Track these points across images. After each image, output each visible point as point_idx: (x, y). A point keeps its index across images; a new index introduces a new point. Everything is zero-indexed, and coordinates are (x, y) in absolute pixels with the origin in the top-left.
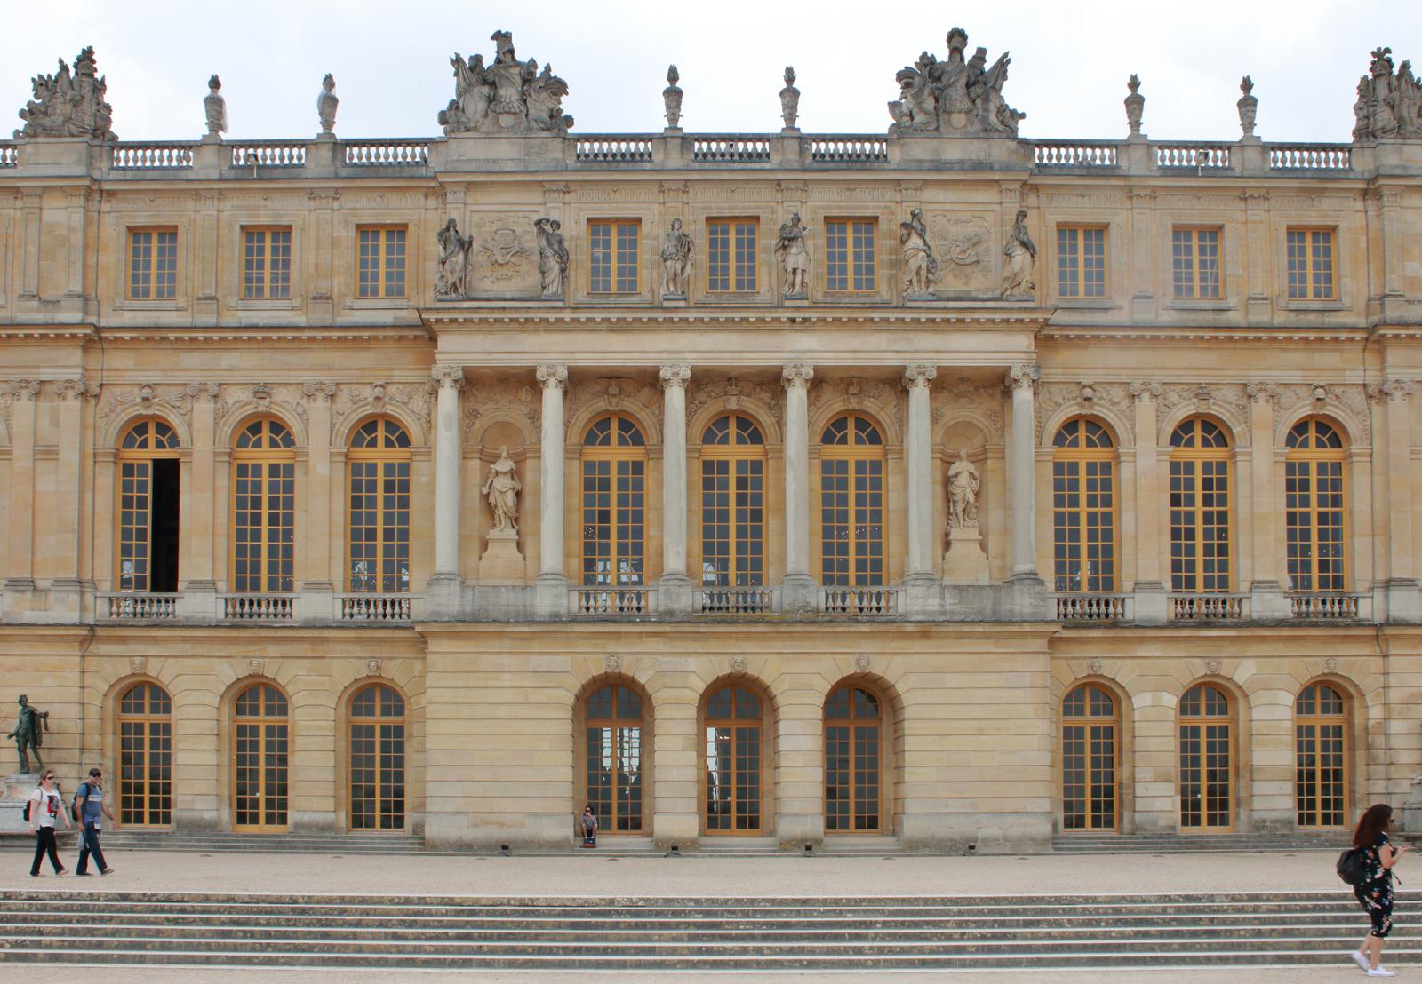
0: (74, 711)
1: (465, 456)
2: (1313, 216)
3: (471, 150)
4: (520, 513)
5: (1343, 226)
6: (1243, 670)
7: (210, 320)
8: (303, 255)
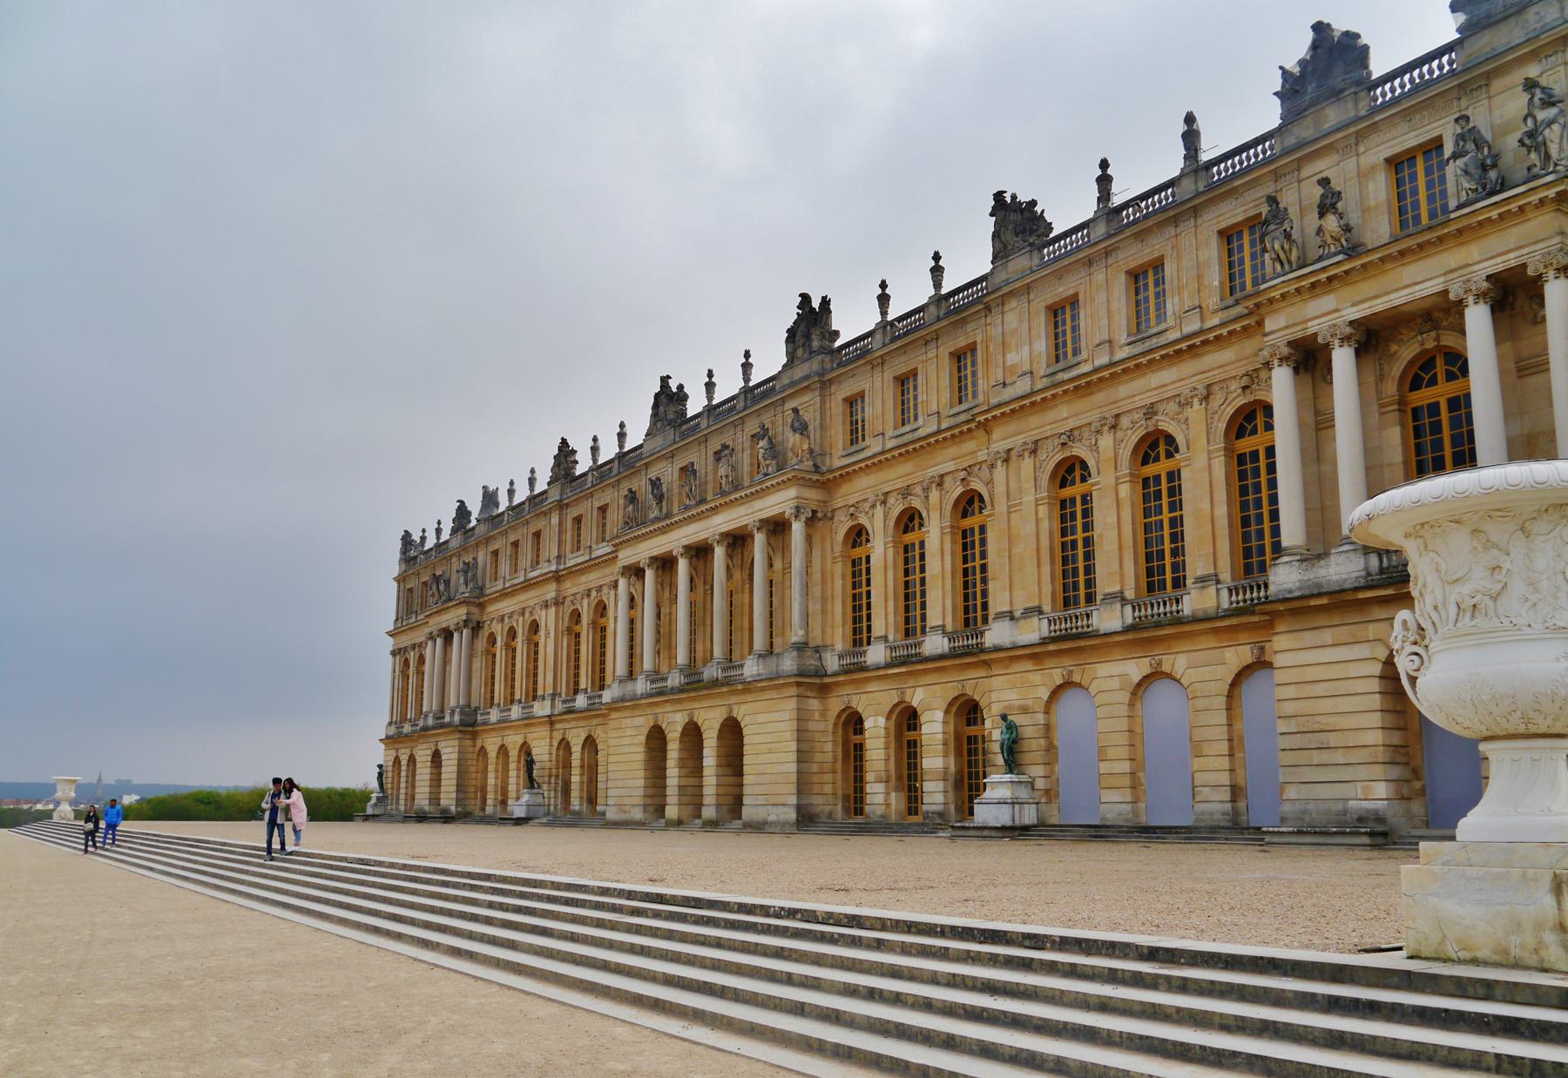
0: (546, 758)
2: (961, 342)
5: (979, 339)
6: (917, 698)
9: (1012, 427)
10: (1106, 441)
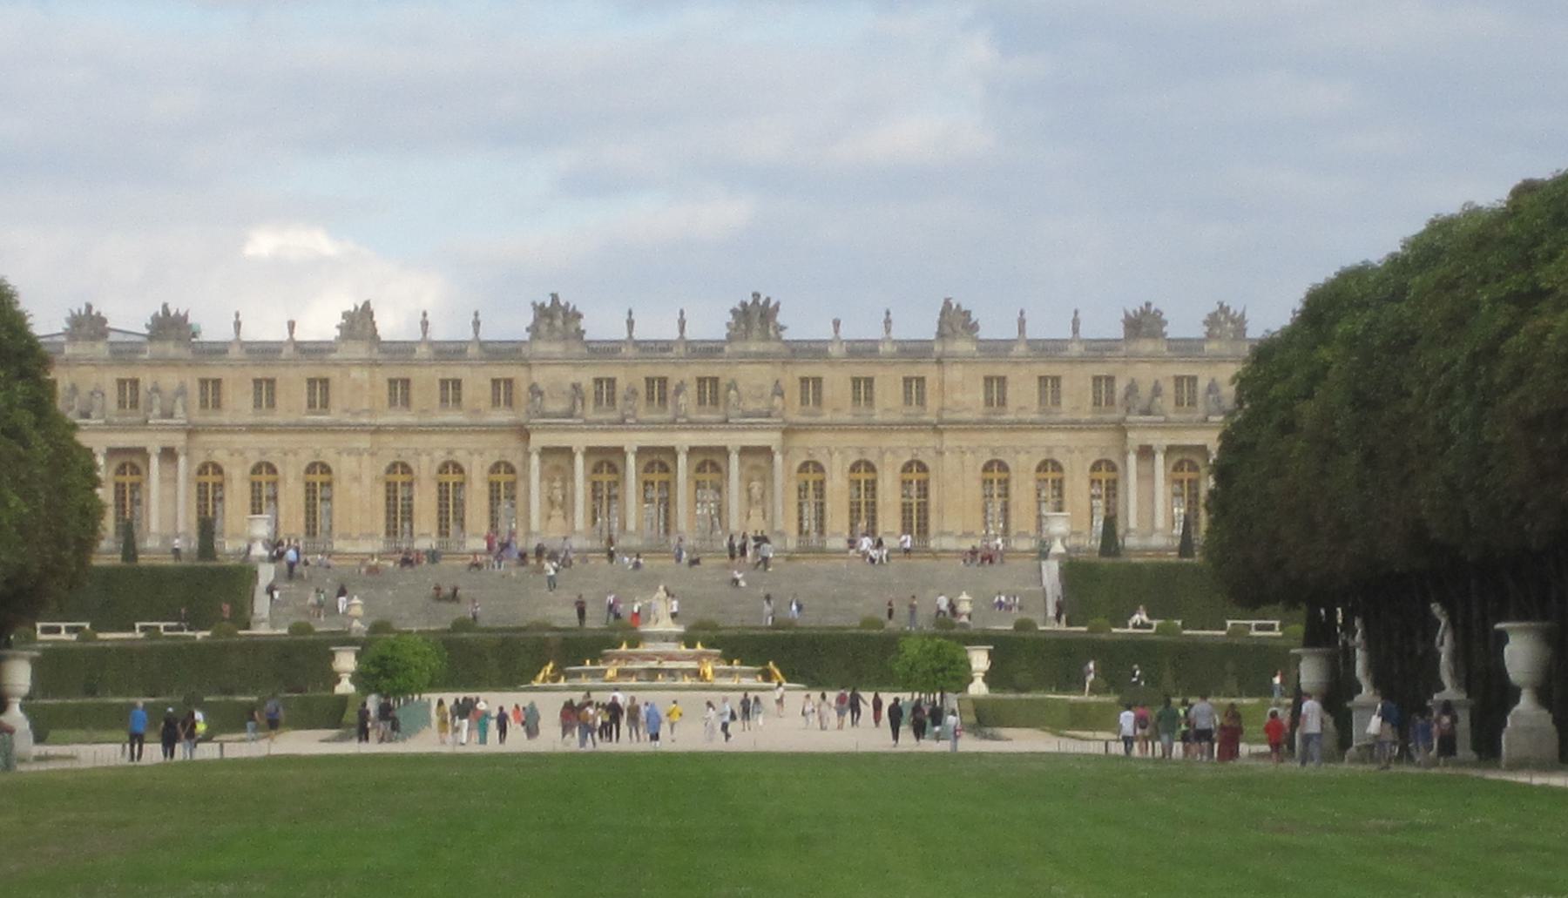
1: (541, 480)
2: (915, 371)
3: (542, 347)
4: (567, 506)
7: (425, 420)
8: (467, 392)
9: (961, 435)
10: (1023, 458)
